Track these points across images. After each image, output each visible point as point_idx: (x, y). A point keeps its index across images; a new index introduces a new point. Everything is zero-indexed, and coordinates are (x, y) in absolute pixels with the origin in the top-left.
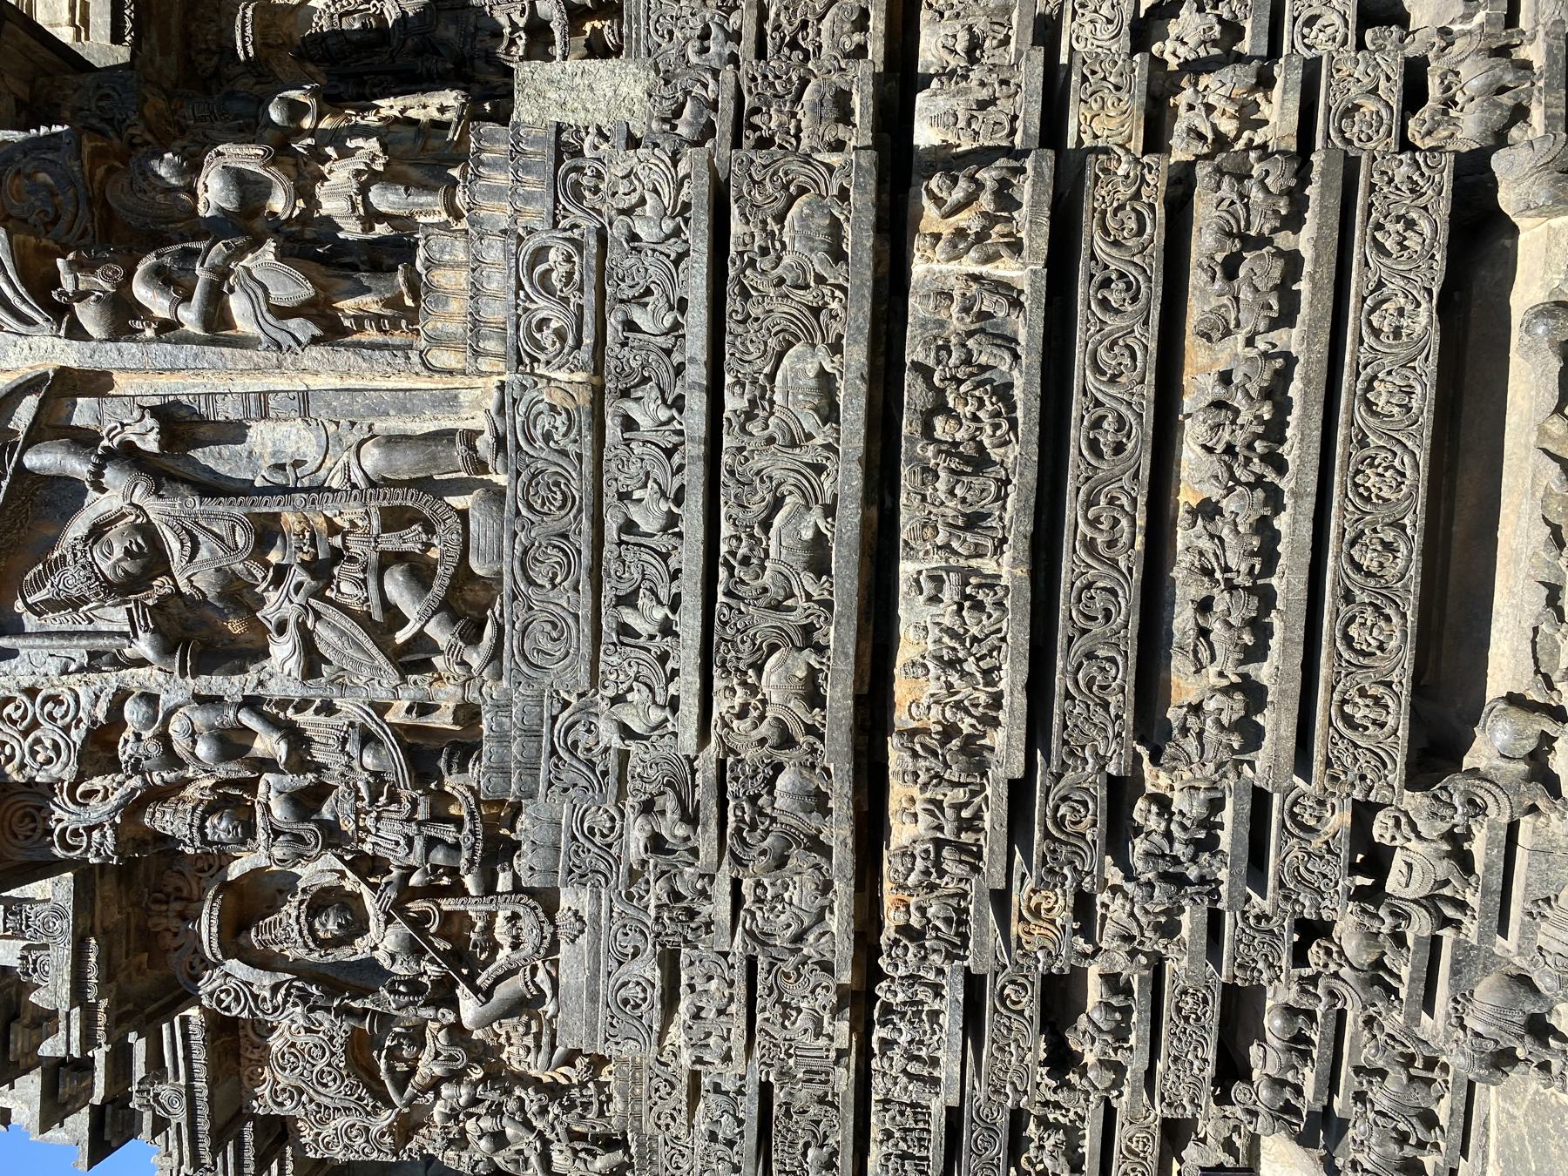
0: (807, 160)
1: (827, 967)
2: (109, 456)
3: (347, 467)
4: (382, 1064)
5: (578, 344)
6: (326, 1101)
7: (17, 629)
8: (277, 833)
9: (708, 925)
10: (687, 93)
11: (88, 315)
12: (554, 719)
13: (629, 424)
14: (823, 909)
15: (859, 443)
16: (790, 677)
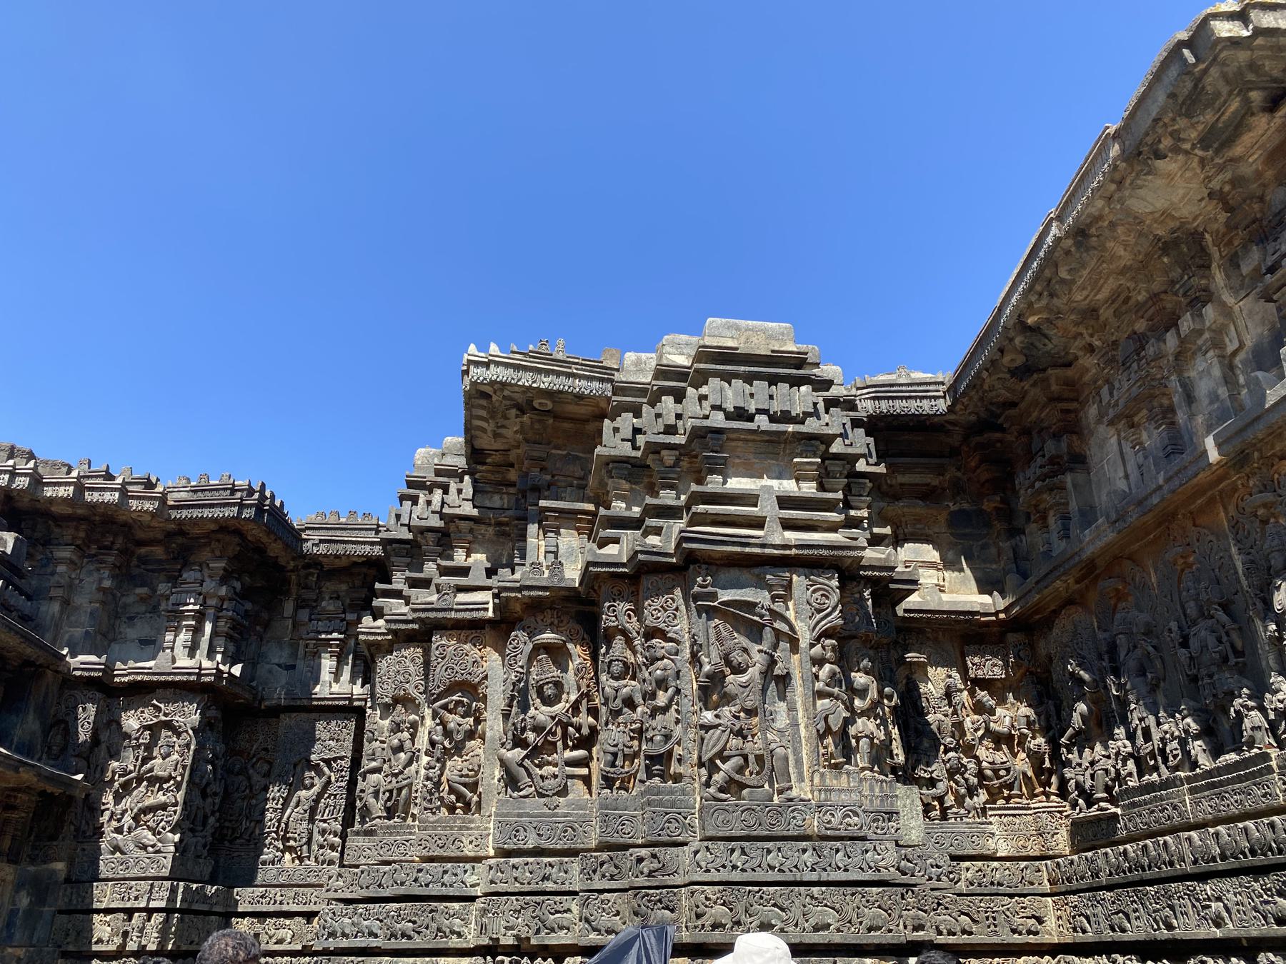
0: (900, 916)
1: (538, 932)
2: (772, 656)
3: (776, 742)
4: (455, 698)
5: (827, 829)
6: (438, 670)
7: (709, 619)
8: (617, 691)
9: (591, 879)
10: (916, 864)
11: (817, 649)
12: (680, 814)
13: (804, 851)
14: (599, 931)
15: (807, 941)
16: (723, 916)
